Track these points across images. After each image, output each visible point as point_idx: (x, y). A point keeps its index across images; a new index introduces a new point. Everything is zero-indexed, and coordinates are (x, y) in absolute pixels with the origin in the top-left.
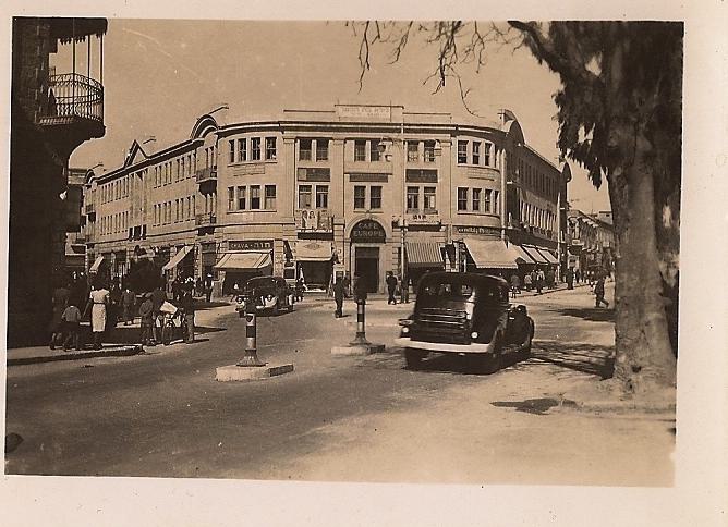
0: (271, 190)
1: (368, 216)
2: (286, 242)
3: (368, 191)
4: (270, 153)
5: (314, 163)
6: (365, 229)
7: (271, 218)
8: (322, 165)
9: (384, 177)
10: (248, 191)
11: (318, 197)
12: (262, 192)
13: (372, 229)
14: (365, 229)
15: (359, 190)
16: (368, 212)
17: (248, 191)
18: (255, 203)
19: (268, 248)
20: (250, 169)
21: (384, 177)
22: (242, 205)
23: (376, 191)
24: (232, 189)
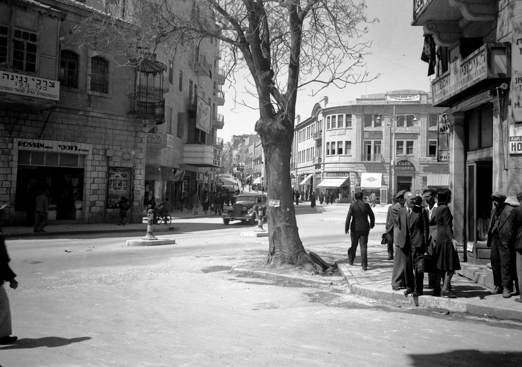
0: (348, 143)
1: (404, 159)
2: (356, 173)
3: (405, 144)
4: (348, 124)
5: (372, 128)
6: (402, 166)
7: (348, 159)
8: (377, 129)
9: (415, 135)
10: (336, 144)
11: (375, 147)
12: (343, 146)
13: (407, 166)
14: (402, 166)
15: (400, 144)
16: (405, 156)
17: (336, 144)
18: (340, 151)
19: (346, 176)
20: (337, 132)
21: (415, 135)
22: (333, 152)
23: (409, 144)
24: (328, 143)
